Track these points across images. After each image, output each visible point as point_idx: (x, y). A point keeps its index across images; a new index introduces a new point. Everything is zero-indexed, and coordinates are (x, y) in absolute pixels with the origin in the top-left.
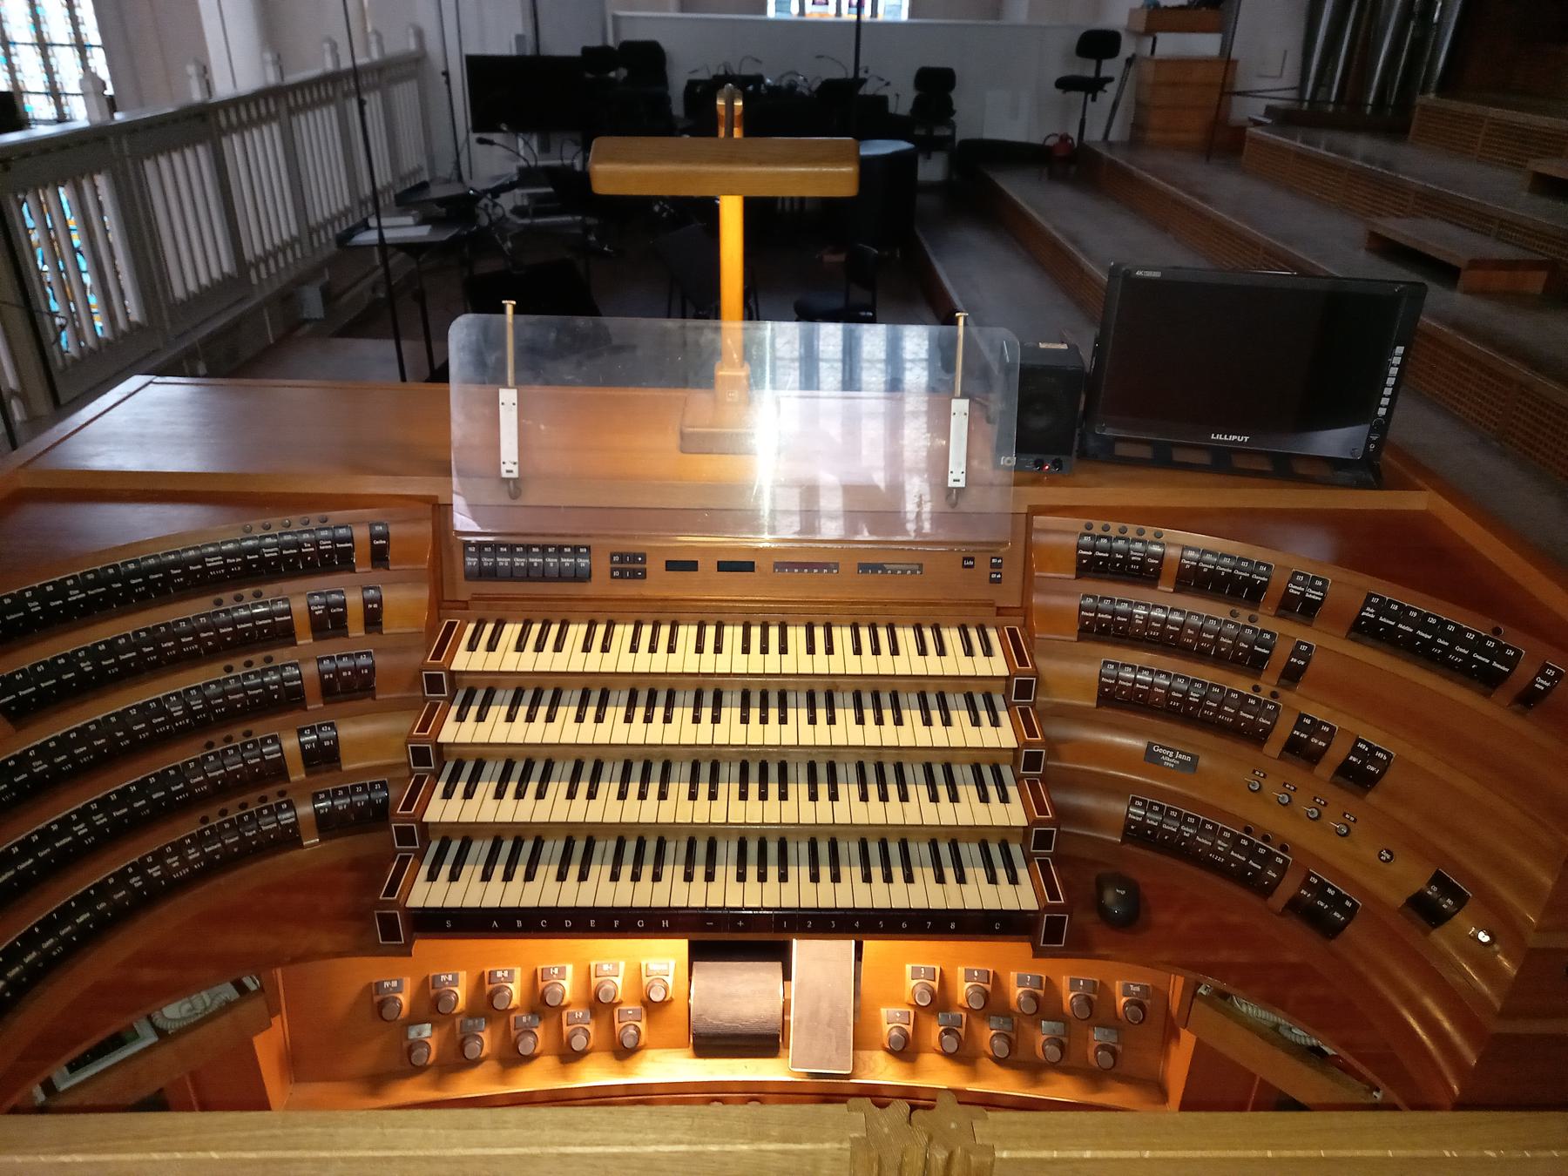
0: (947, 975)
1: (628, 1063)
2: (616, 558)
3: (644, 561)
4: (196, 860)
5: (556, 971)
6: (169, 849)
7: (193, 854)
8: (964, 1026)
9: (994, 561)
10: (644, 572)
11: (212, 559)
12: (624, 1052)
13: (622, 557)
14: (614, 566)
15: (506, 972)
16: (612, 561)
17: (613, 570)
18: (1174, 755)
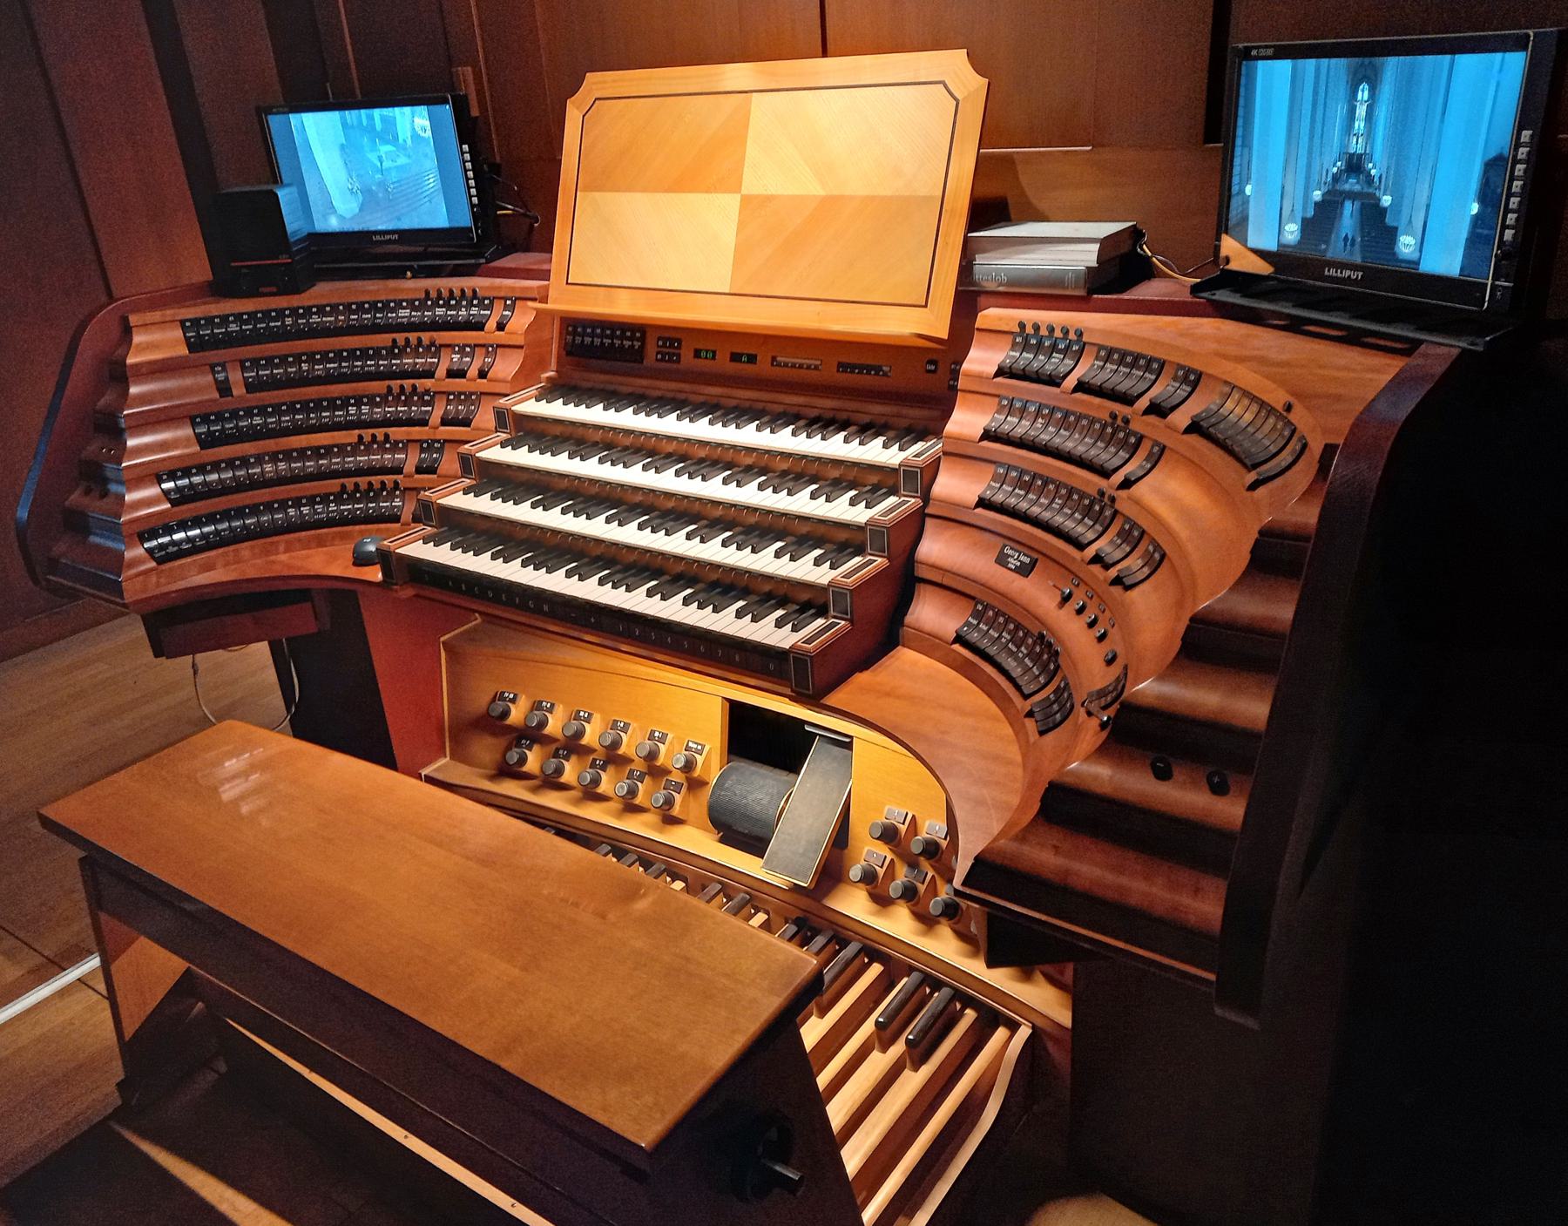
0: (919, 821)
1: (669, 827)
2: (660, 343)
3: (679, 347)
4: (333, 511)
5: (622, 725)
6: (318, 499)
7: (333, 507)
8: (926, 883)
9: (953, 366)
10: (679, 356)
11: (404, 311)
12: (670, 821)
13: (665, 339)
14: (659, 349)
15: (587, 714)
16: (658, 346)
17: (658, 353)
18: (1018, 556)
